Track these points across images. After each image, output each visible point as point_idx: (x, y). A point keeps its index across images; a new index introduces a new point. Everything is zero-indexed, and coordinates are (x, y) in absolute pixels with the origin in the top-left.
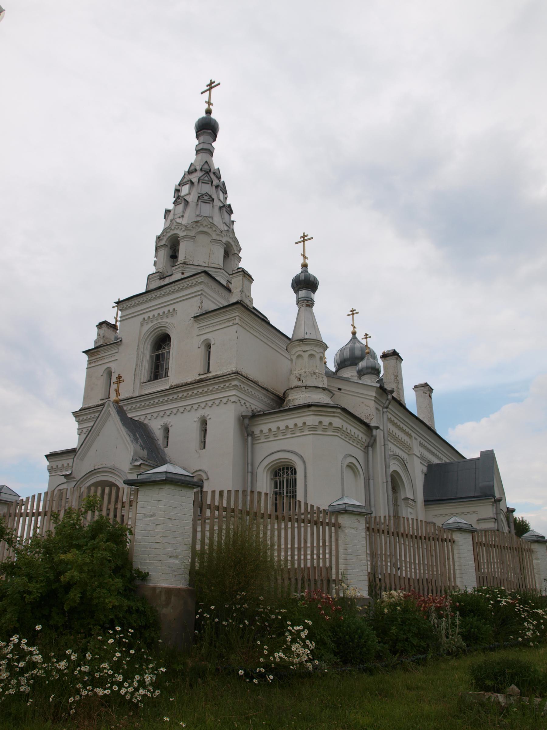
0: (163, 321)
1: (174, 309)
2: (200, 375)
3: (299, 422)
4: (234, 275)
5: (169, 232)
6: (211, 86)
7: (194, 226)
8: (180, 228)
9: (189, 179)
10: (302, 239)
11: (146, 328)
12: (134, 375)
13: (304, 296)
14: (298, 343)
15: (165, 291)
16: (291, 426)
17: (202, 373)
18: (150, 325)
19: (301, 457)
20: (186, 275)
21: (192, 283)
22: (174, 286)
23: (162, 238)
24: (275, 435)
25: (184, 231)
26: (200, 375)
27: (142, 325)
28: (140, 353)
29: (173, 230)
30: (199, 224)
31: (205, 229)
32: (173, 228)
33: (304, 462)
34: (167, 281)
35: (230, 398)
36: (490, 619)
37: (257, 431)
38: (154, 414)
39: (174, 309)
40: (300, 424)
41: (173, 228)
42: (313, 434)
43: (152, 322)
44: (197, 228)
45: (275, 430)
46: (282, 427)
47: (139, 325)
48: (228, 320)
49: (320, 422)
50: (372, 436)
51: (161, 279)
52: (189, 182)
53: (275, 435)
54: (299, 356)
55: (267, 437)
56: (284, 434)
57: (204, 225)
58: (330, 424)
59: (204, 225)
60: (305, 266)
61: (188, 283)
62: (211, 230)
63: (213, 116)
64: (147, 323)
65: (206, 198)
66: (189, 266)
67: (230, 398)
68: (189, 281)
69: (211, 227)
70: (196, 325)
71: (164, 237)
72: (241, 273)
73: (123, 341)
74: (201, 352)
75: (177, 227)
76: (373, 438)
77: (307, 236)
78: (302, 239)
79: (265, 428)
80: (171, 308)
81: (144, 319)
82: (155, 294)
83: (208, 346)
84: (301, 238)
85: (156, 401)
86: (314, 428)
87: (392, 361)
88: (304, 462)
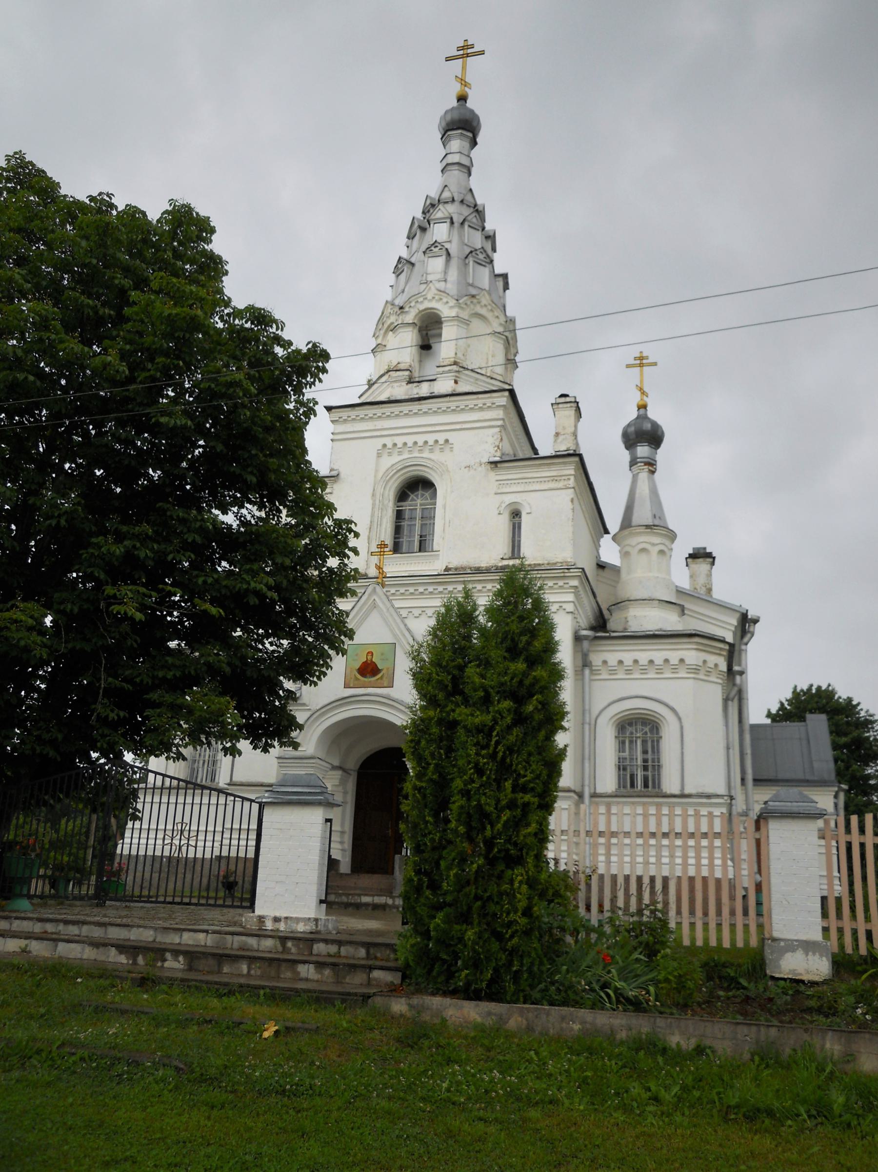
0: (424, 455)
1: (447, 441)
2: (502, 559)
3: (674, 657)
4: (560, 406)
5: (422, 302)
6: (466, 51)
7: (469, 303)
8: (445, 300)
9: (447, 215)
10: (638, 362)
11: (388, 462)
12: (369, 538)
13: (646, 455)
14: (642, 529)
15: (430, 406)
16: (659, 661)
17: (506, 557)
18: (396, 458)
19: (672, 709)
20: (463, 388)
21: (484, 404)
22: (449, 402)
23: (407, 309)
24: (628, 671)
25: (451, 307)
26: (502, 559)
27: (379, 455)
28: (377, 502)
29: (430, 301)
30: (475, 301)
31: (483, 311)
32: (429, 297)
33: (680, 719)
34: (424, 390)
35: (565, 606)
36: (873, 960)
37: (596, 659)
38: (413, 610)
39: (447, 441)
40: (674, 661)
41: (429, 297)
42: (694, 678)
43: (400, 453)
44: (472, 306)
45: (631, 663)
46: (628, 662)
47: (375, 455)
48: (554, 479)
49: (705, 662)
50: (734, 685)
51: (410, 382)
52: (448, 220)
53: (628, 671)
54: (643, 550)
55: (613, 672)
56: (644, 671)
57: (483, 304)
58: (666, 661)
59: (483, 304)
60: (643, 407)
61: (475, 402)
62: (491, 314)
63: (470, 104)
64: (390, 454)
65: (481, 256)
66: (467, 372)
67: (565, 606)
68: (478, 399)
69: (492, 310)
70: (493, 476)
71: (412, 310)
72: (572, 404)
73: (342, 475)
74: (503, 524)
75: (437, 297)
76: (736, 689)
77: (647, 358)
78: (638, 362)
79: (612, 658)
80: (441, 438)
81: (385, 446)
82: (410, 408)
83: (516, 514)
84: (635, 359)
85: (421, 589)
86: (696, 670)
87: (702, 566)
88: (680, 719)
